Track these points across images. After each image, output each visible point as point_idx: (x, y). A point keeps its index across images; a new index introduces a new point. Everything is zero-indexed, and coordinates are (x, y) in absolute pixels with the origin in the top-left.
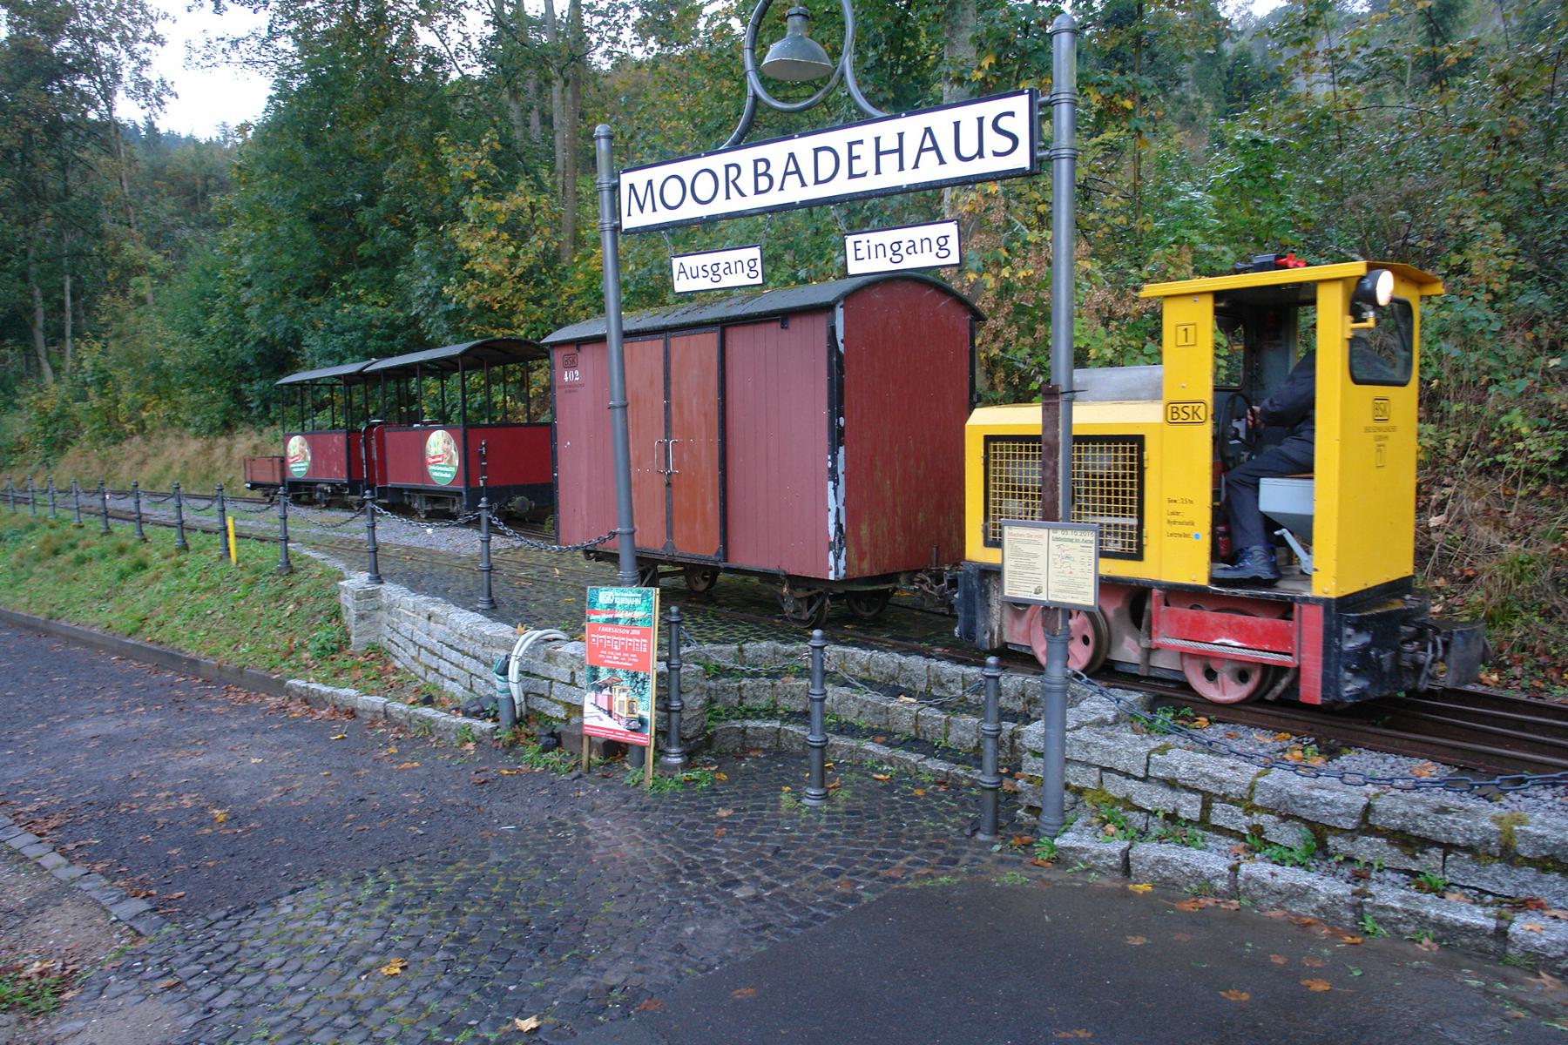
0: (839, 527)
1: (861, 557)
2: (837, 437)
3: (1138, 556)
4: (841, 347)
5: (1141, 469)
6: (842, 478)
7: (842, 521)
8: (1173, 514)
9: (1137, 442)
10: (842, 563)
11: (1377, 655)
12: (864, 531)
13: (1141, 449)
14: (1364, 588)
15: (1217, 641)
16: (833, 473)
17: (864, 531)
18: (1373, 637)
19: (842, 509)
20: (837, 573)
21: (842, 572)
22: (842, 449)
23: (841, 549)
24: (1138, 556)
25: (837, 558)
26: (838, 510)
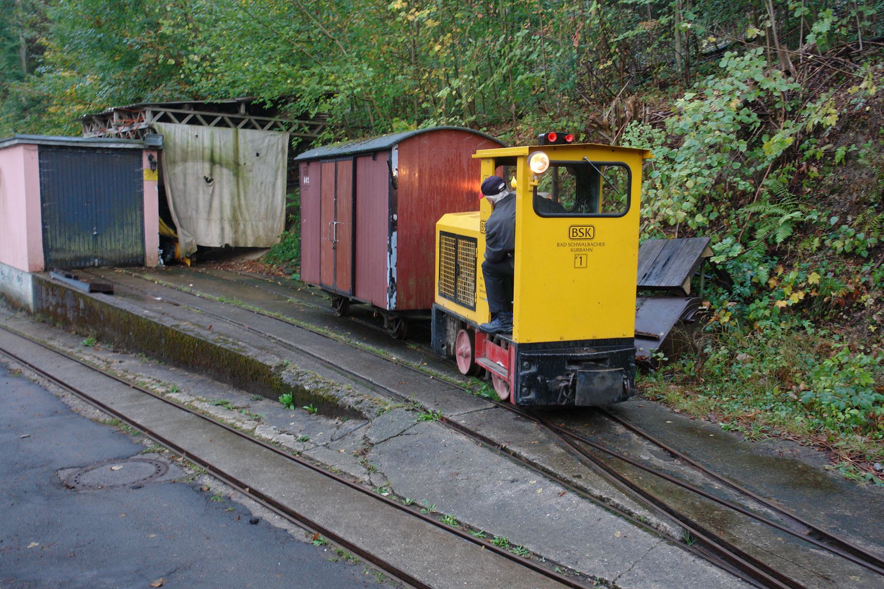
0: (392, 279)
1: (409, 298)
2: (393, 226)
3: (473, 309)
4: (395, 173)
5: (476, 259)
6: (394, 251)
7: (394, 275)
9: (474, 240)
10: (394, 300)
11: (543, 380)
12: (412, 282)
13: (476, 246)
14: (559, 340)
15: (498, 363)
16: (390, 246)
17: (412, 282)
18: (539, 369)
19: (394, 269)
20: (390, 306)
21: (393, 306)
22: (395, 234)
23: (393, 292)
24: (473, 309)
25: (391, 297)
26: (391, 269)
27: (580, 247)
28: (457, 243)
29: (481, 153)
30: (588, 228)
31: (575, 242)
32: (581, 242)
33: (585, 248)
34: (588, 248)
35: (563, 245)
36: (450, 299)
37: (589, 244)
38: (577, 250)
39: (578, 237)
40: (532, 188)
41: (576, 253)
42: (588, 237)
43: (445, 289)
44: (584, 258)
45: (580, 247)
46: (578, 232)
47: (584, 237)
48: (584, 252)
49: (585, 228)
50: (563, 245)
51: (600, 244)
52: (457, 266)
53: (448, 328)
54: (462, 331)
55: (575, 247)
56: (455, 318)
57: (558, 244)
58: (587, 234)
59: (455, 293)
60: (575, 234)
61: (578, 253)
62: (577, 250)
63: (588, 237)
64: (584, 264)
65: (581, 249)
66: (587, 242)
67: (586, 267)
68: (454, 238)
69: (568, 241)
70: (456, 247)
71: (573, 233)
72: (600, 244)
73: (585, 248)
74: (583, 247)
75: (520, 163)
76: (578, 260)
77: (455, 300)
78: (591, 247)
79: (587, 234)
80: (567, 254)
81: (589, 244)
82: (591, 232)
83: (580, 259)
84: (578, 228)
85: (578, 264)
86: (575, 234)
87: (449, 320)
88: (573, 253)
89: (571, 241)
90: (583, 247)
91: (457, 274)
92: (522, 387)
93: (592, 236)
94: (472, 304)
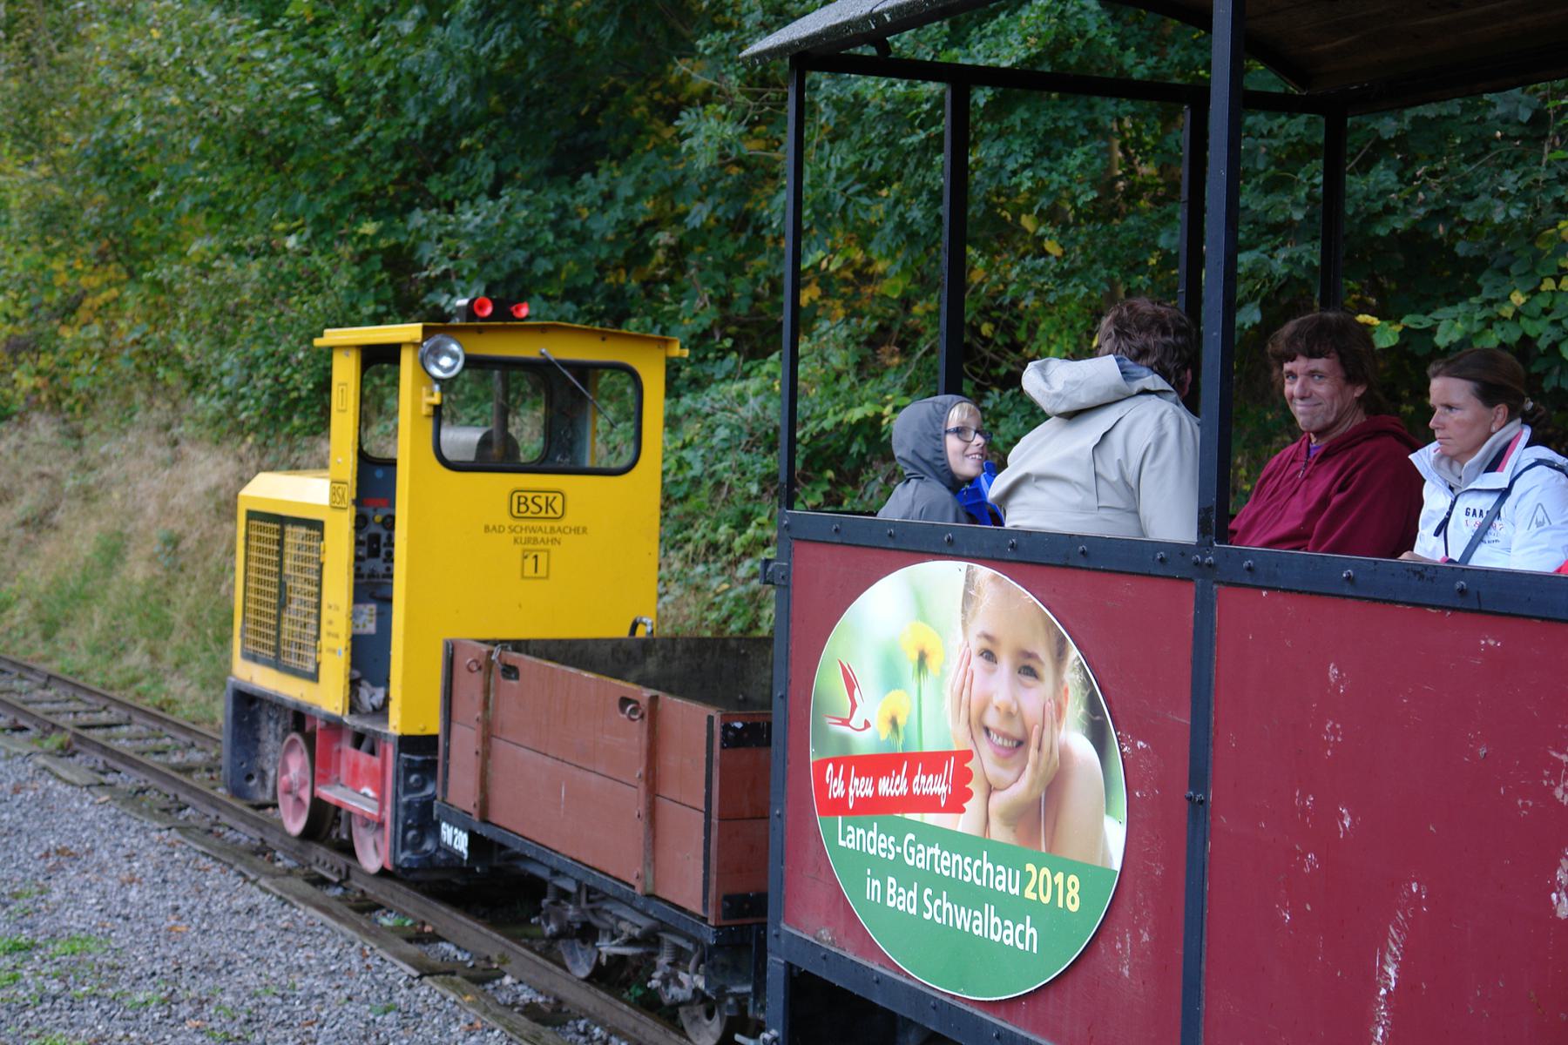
3: (314, 677)
5: (321, 565)
8: (330, 623)
24: (314, 677)
27: (533, 535)
28: (282, 533)
29: (332, 336)
30: (551, 496)
31: (524, 523)
32: (536, 523)
35: (498, 529)
36: (267, 663)
38: (528, 541)
39: (529, 514)
40: (430, 410)
41: (530, 546)
42: (551, 514)
43: (256, 643)
44: (542, 557)
45: (533, 535)
47: (543, 514)
48: (542, 546)
50: (498, 529)
51: (576, 530)
52: (282, 586)
53: (263, 735)
54: (294, 736)
55: (524, 535)
56: (275, 705)
57: (487, 529)
58: (550, 510)
59: (277, 649)
60: (523, 508)
61: (530, 546)
62: (528, 541)
63: (551, 514)
64: (542, 571)
65: (535, 540)
66: (548, 524)
67: (547, 577)
68: (277, 522)
69: (508, 521)
70: (281, 543)
71: (519, 505)
72: (576, 530)
74: (539, 535)
75: (407, 360)
76: (530, 562)
77: (277, 664)
78: (558, 536)
79: (550, 510)
82: (558, 505)
83: (534, 560)
84: (530, 496)
86: (523, 508)
87: (263, 717)
88: (519, 548)
89: (514, 523)
90: (539, 535)
91: (283, 604)
92: (406, 829)
93: (560, 512)
94: (311, 667)
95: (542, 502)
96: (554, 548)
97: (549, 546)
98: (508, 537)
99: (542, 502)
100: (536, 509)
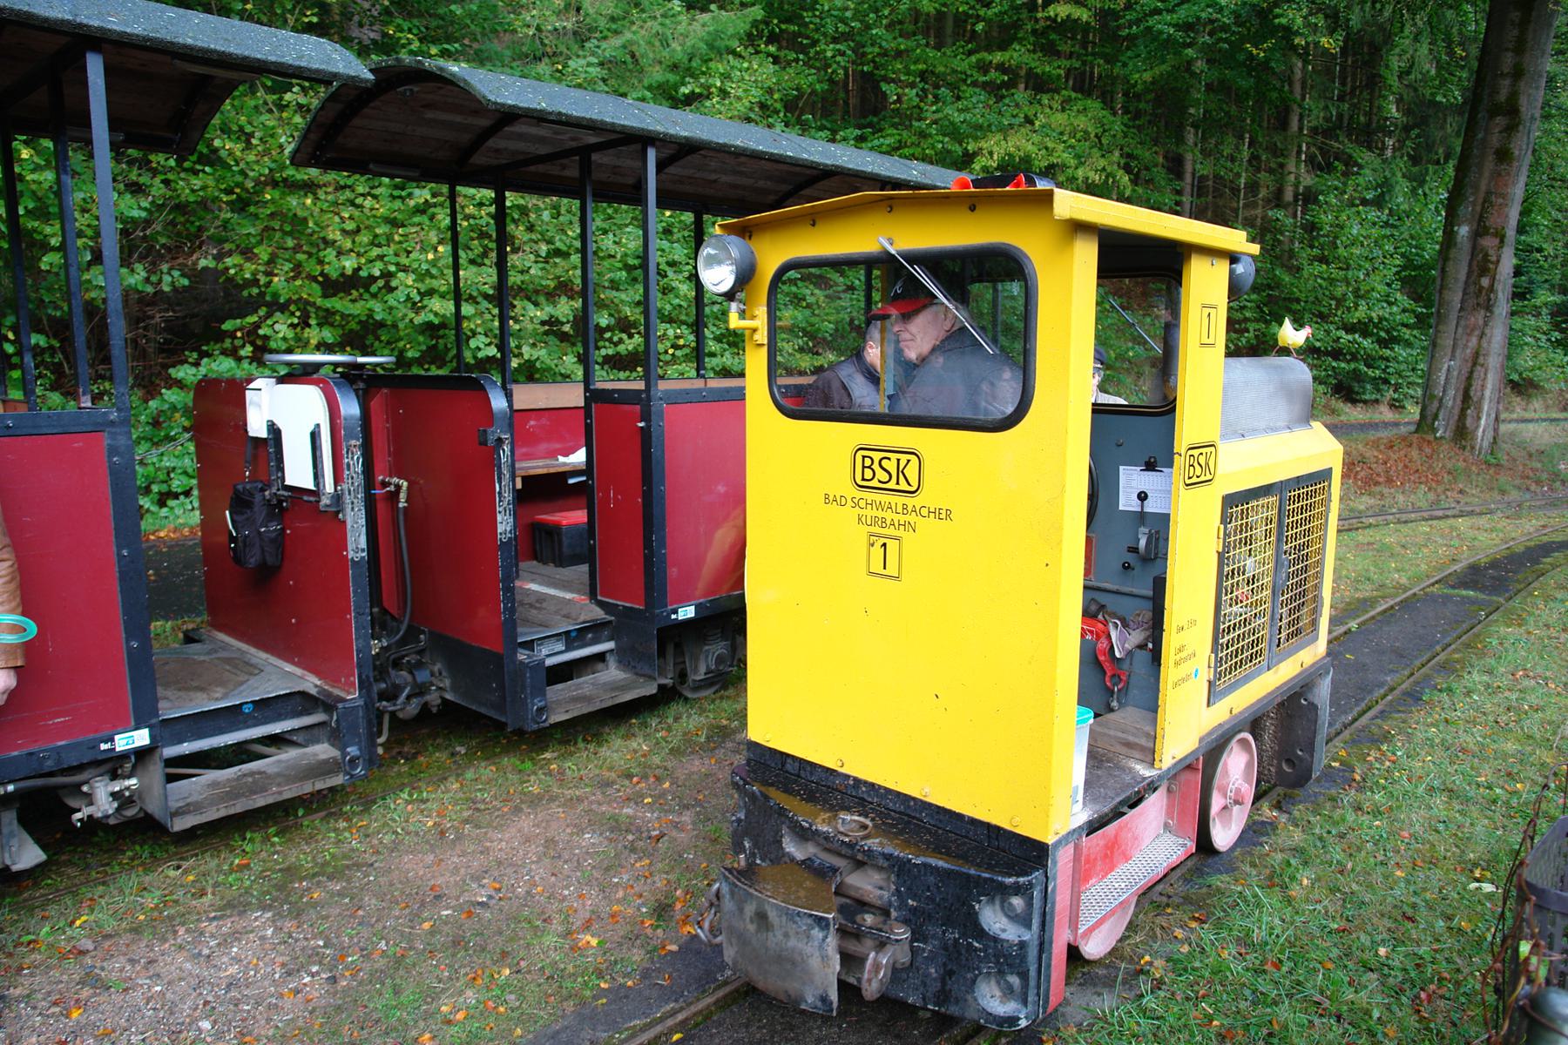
27: (880, 514)
30: (904, 458)
33: (896, 517)
34: (903, 518)
37: (905, 507)
38: (875, 521)
39: (875, 483)
45: (880, 514)
46: (876, 466)
47: (892, 485)
49: (894, 456)
51: (937, 513)
55: (870, 512)
57: (827, 497)
63: (903, 486)
64: (892, 569)
65: (884, 520)
66: (899, 500)
69: (854, 492)
72: (937, 513)
73: (896, 517)
74: (889, 515)
76: (877, 551)
78: (912, 518)
80: (848, 530)
81: (905, 507)
82: (911, 472)
84: (877, 456)
85: (877, 566)
90: (889, 515)
95: (891, 466)
96: (905, 535)
97: (900, 533)
98: (851, 513)
99: (891, 466)
100: (884, 477)
